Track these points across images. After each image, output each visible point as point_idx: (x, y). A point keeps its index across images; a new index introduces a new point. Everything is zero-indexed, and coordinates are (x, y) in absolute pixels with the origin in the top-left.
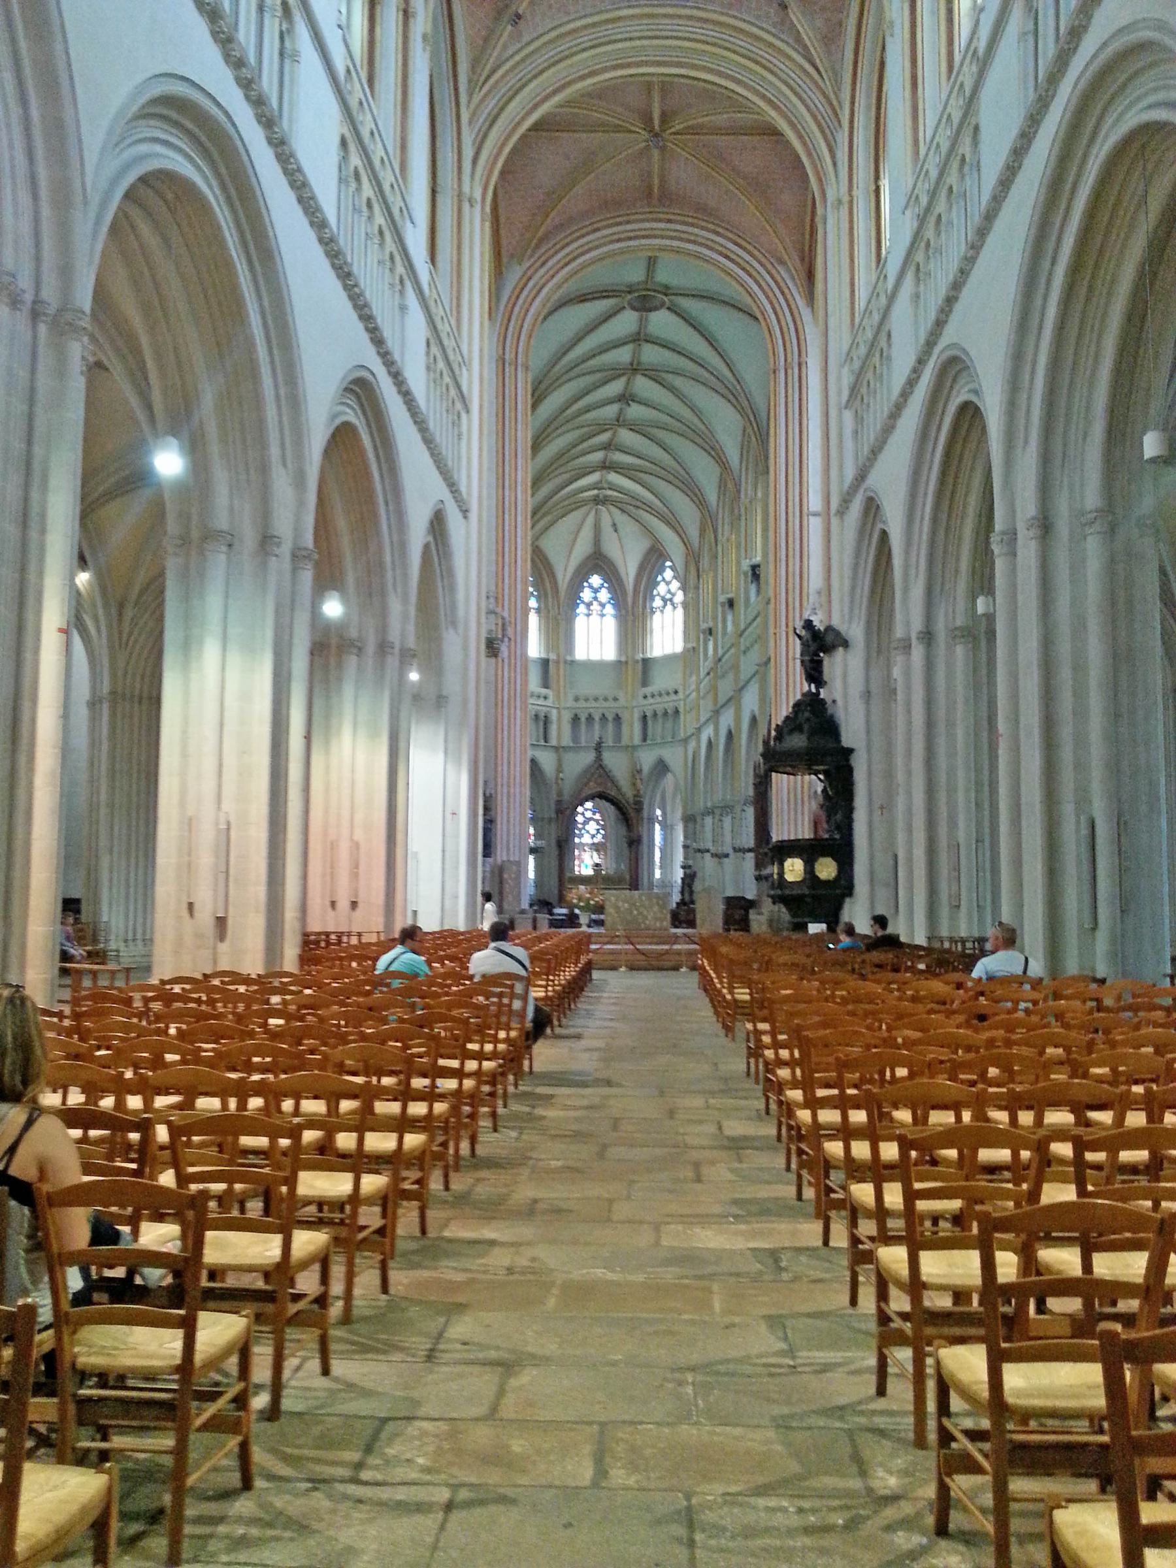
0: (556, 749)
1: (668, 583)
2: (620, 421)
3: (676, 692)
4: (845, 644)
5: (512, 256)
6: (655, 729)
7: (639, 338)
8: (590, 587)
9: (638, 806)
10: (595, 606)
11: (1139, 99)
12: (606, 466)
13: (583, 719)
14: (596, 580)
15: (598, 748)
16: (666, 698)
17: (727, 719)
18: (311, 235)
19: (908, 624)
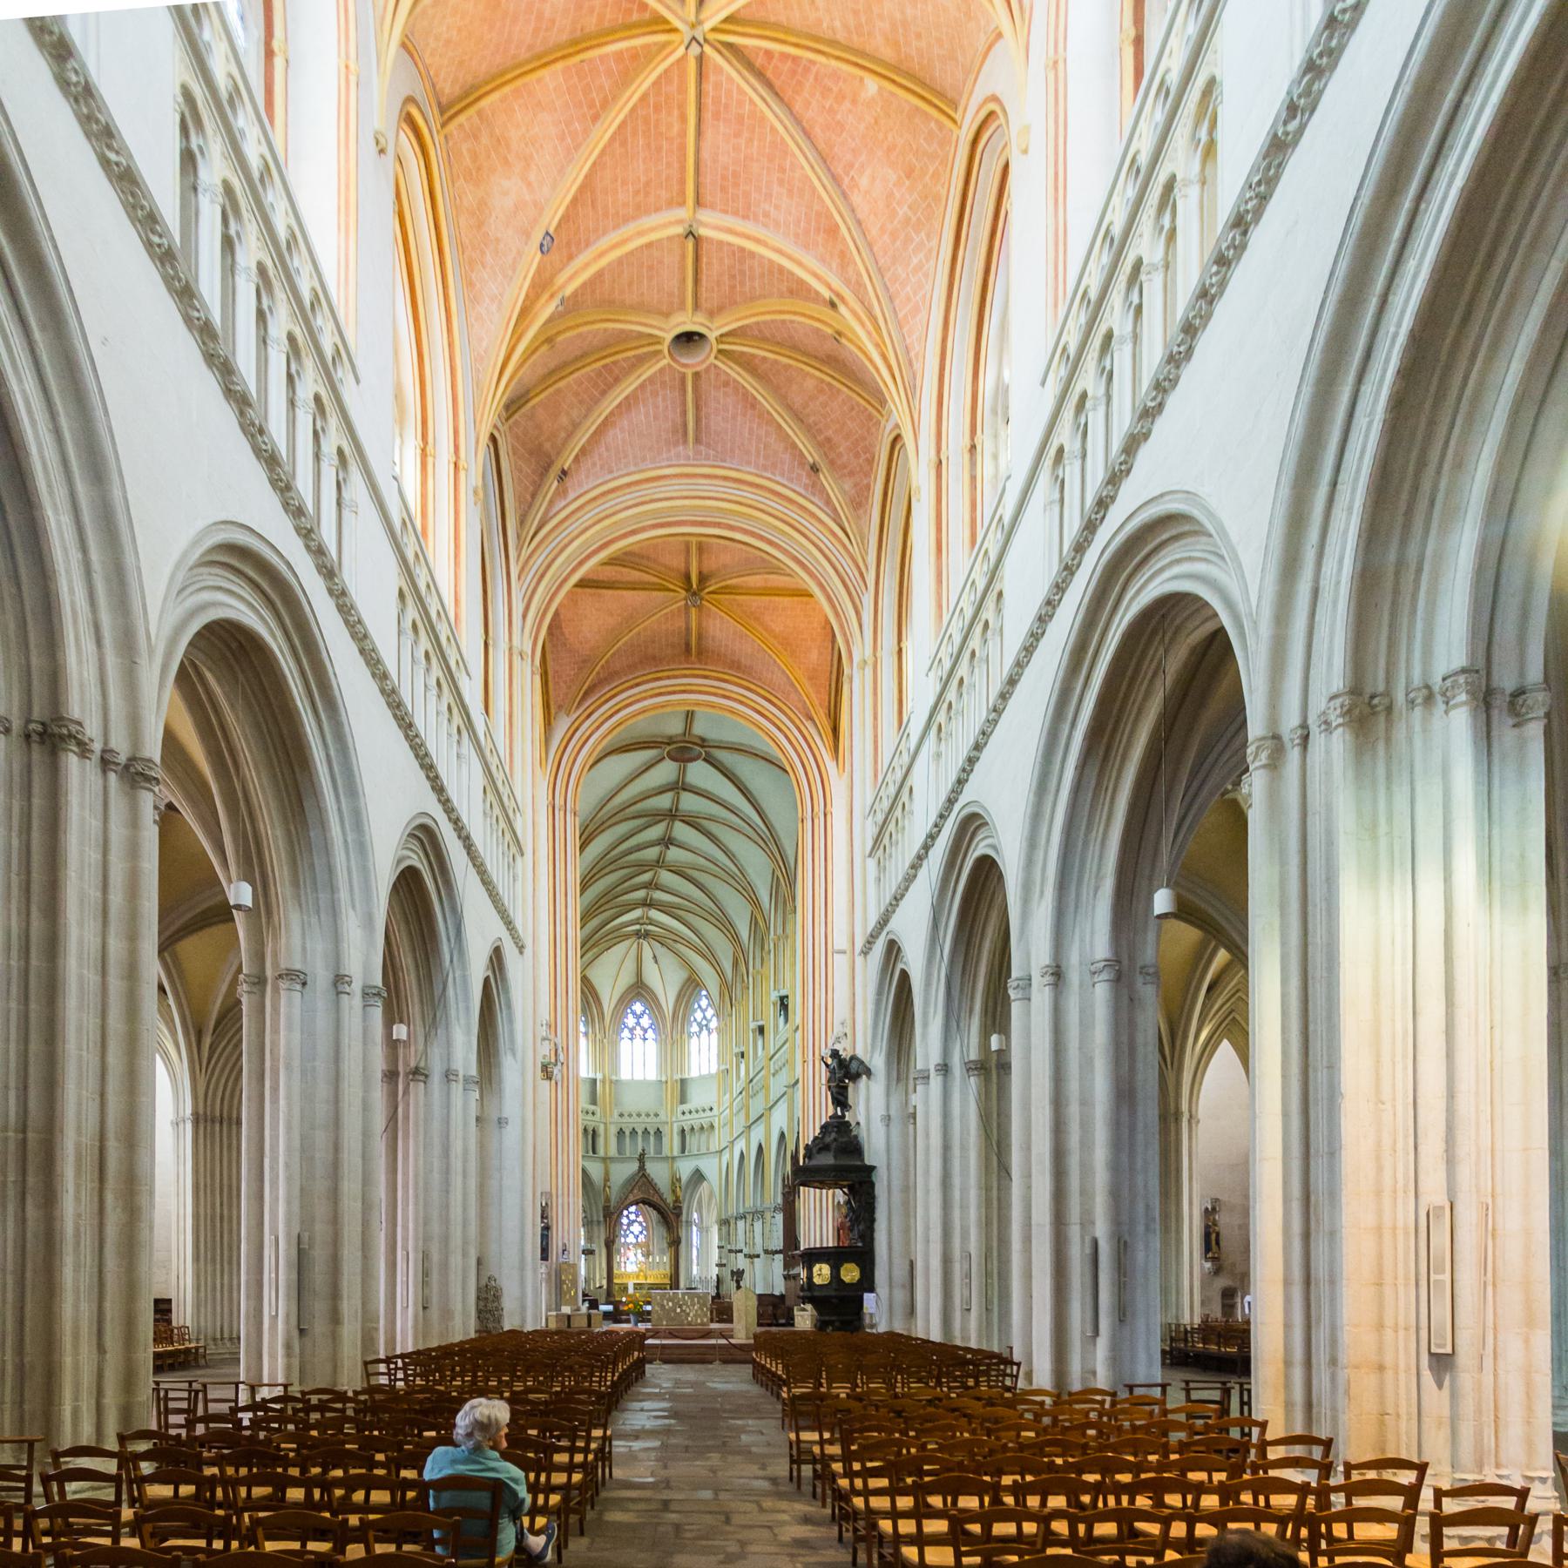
1: (704, 1011)
2: (659, 863)
4: (868, 1072)
5: (560, 707)
6: (692, 1141)
7: (679, 786)
8: (634, 1013)
9: (678, 1211)
10: (638, 1031)
11: (1162, 570)
12: (647, 904)
13: (627, 1133)
15: (642, 1159)
16: (702, 1114)
17: (757, 1134)
18: (373, 687)
19: (926, 1056)
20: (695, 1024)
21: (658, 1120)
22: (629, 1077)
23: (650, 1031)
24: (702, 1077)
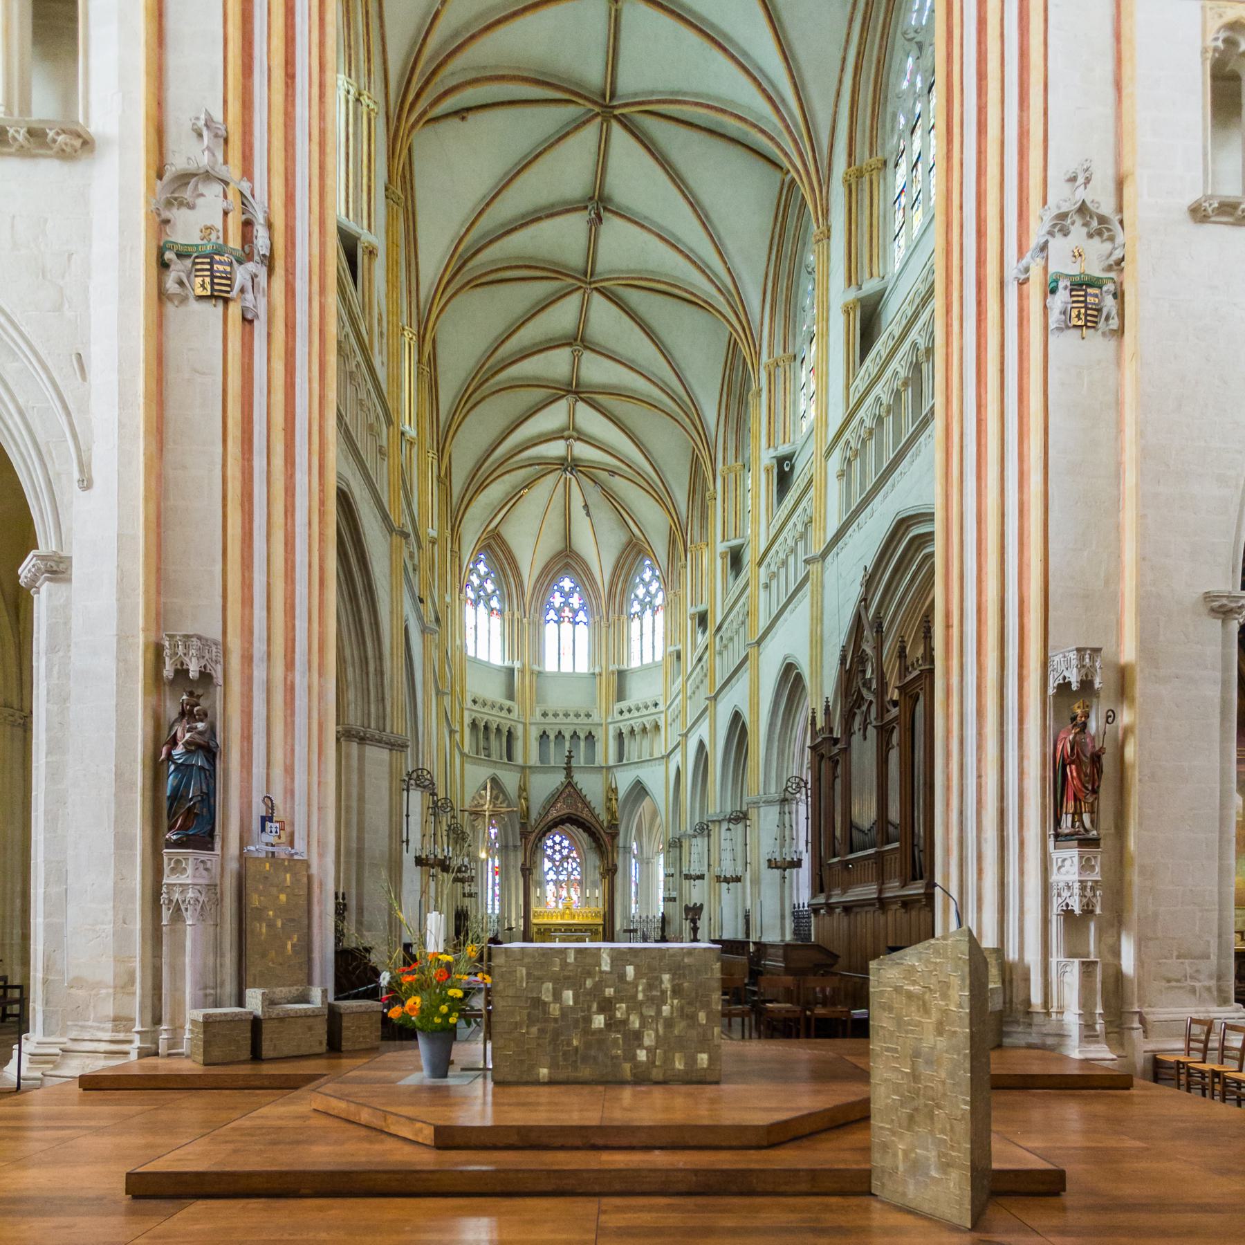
0: (523, 769)
1: (647, 584)
3: (656, 705)
6: (632, 748)
8: (561, 590)
13: (552, 737)
14: (567, 584)
15: (568, 770)
20: (635, 603)
21: (590, 721)
23: (581, 613)
24: (644, 668)
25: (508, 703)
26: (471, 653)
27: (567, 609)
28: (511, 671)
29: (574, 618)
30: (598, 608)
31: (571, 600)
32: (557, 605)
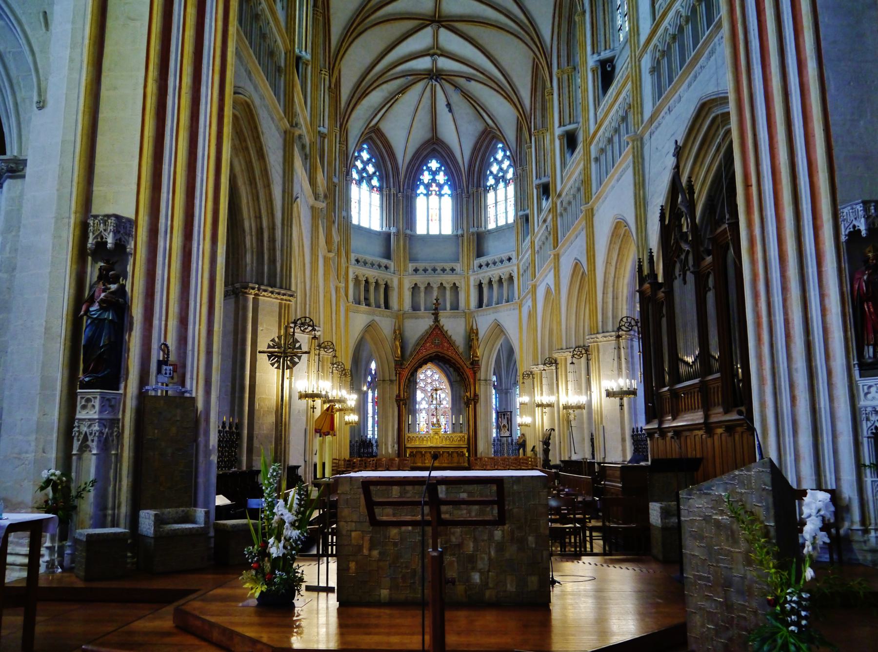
1: (500, 163)
3: (509, 259)
8: (429, 169)
10: (434, 187)
13: (422, 289)
14: (434, 164)
20: (491, 178)
22: (425, 233)
24: (499, 229)
25: (384, 261)
26: (355, 221)
27: (434, 185)
28: (388, 235)
29: (440, 191)
30: (459, 183)
31: (437, 177)
32: (426, 182)
